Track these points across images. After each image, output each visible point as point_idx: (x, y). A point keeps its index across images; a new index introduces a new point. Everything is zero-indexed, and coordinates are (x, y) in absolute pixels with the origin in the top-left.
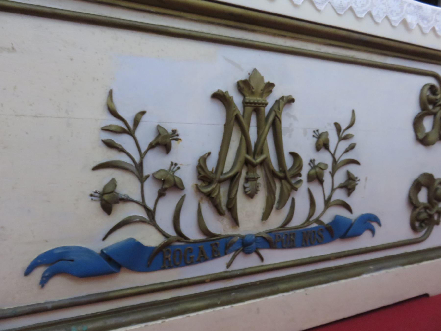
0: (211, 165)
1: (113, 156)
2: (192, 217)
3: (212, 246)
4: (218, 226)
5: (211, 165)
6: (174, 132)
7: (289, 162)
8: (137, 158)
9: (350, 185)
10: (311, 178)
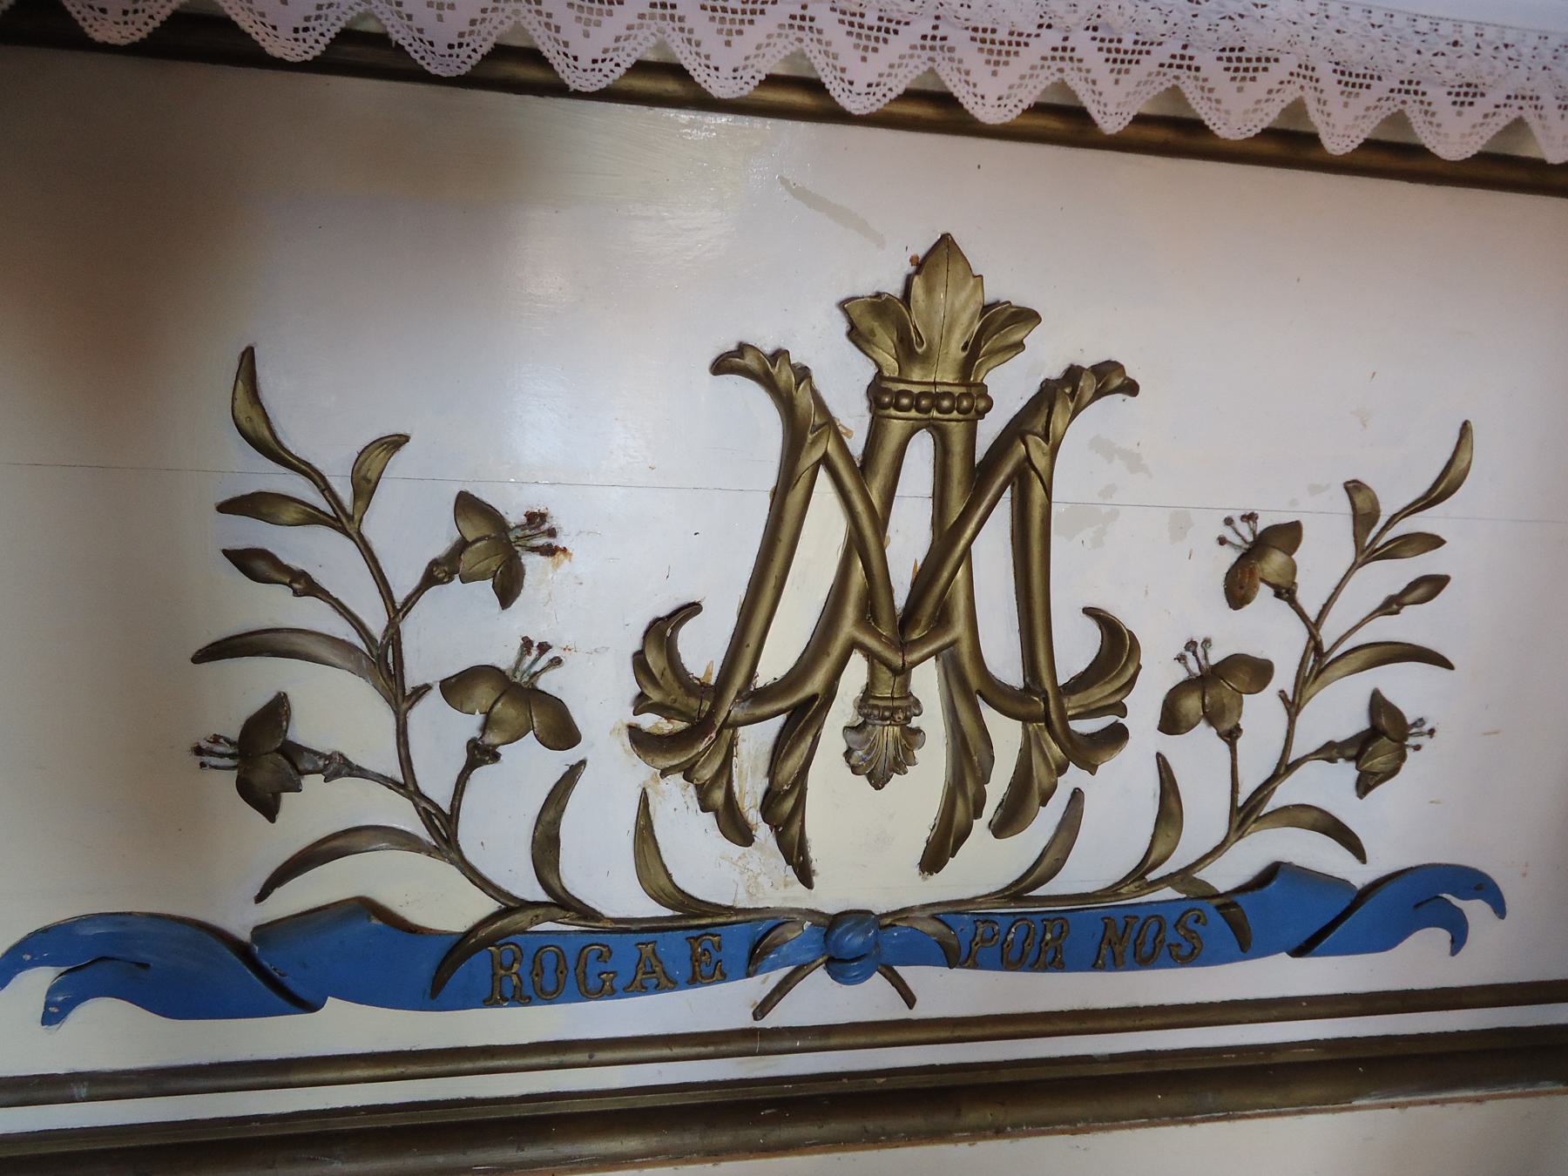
0: (702, 651)
1: (276, 607)
3: (698, 939)
5: (702, 651)
6: (535, 519)
7: (1074, 648)
8: (377, 622)
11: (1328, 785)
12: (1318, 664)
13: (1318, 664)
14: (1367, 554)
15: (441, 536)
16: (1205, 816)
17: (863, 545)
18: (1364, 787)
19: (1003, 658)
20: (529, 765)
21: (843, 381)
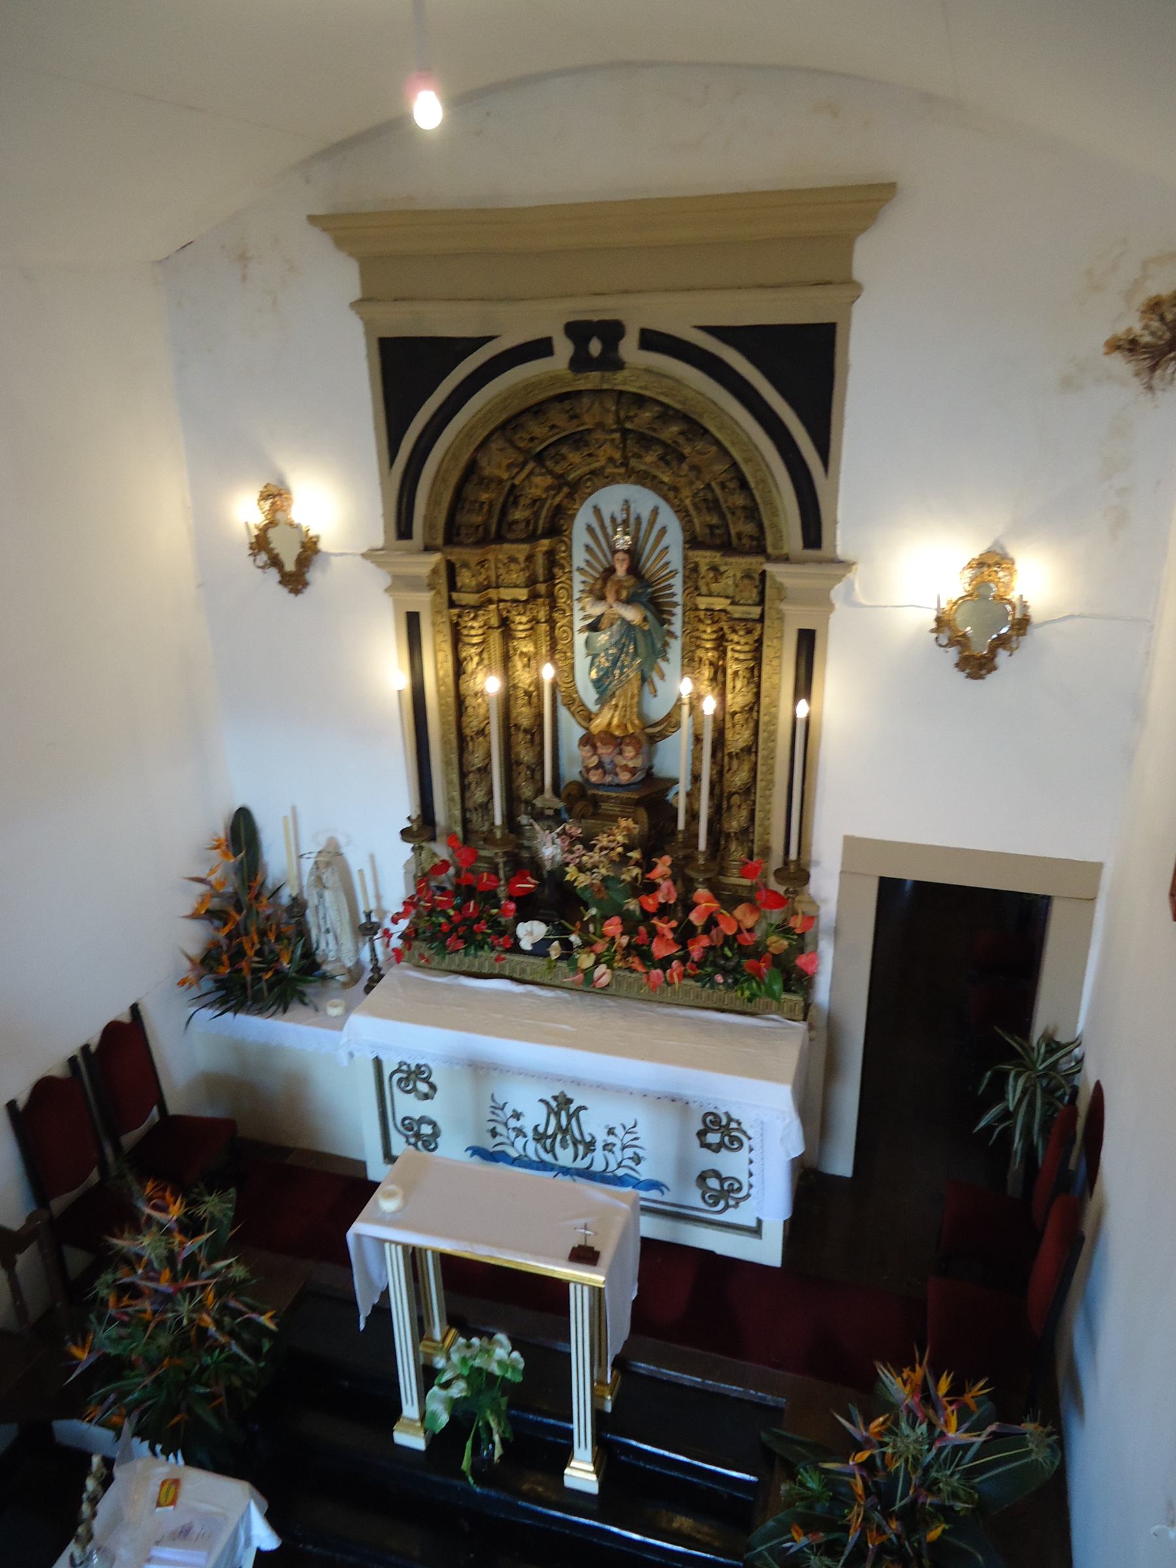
0: (541, 1129)
1: (494, 1117)
2: (533, 1150)
4: (548, 1158)
7: (588, 1139)
9: (638, 1160)
10: (605, 1147)
11: (632, 1164)
12: (624, 1148)
13: (624, 1148)
15: (511, 1113)
17: (559, 1121)
21: (554, 1104)
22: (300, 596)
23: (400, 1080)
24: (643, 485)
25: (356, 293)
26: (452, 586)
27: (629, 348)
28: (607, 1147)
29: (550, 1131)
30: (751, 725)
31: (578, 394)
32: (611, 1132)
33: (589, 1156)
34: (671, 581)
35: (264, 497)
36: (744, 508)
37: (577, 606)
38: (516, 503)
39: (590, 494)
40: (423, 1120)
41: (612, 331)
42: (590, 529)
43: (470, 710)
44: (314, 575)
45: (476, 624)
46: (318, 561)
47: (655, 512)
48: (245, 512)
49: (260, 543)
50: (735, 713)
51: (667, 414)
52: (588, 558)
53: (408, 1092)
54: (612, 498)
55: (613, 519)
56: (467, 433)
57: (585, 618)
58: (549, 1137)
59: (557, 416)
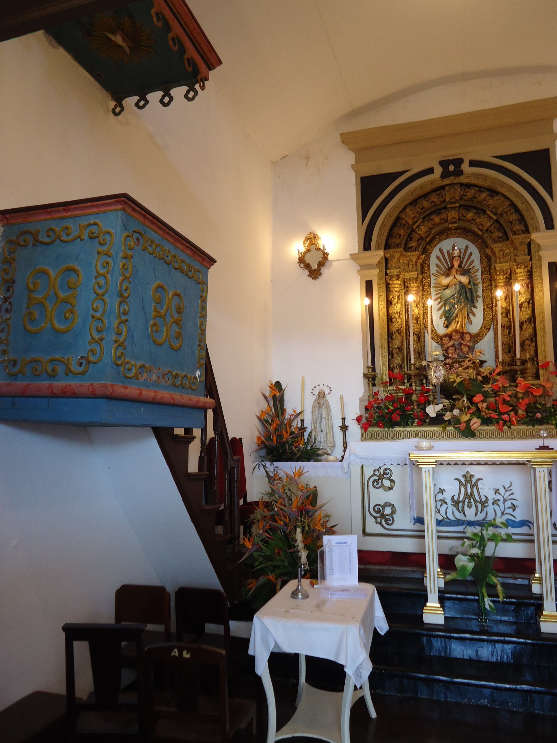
0: (456, 498)
2: (452, 513)
3: (458, 522)
4: (460, 516)
7: (484, 499)
9: (514, 508)
11: (510, 511)
12: (505, 501)
13: (505, 501)
14: (506, 491)
15: (438, 490)
16: (499, 514)
18: (514, 511)
19: (477, 498)
20: (445, 506)
21: (463, 480)
22: (317, 280)
23: (375, 481)
24: (462, 237)
25: (353, 162)
26: (386, 268)
27: (465, 166)
28: (495, 502)
29: (461, 498)
30: (531, 309)
31: (443, 187)
32: (497, 491)
33: (485, 509)
34: (476, 274)
35: (307, 239)
36: (518, 219)
37: (433, 290)
38: (411, 239)
39: (438, 243)
40: (387, 504)
41: (458, 162)
42: (438, 258)
43: (394, 320)
44: (324, 270)
45: (397, 282)
46: (327, 264)
47: (467, 247)
48: (297, 247)
49: (301, 260)
50: (523, 302)
51: (481, 189)
52: (437, 269)
53: (379, 488)
54: (446, 245)
55: (448, 252)
56: (395, 207)
57: (436, 295)
58: (461, 502)
59: (434, 198)
